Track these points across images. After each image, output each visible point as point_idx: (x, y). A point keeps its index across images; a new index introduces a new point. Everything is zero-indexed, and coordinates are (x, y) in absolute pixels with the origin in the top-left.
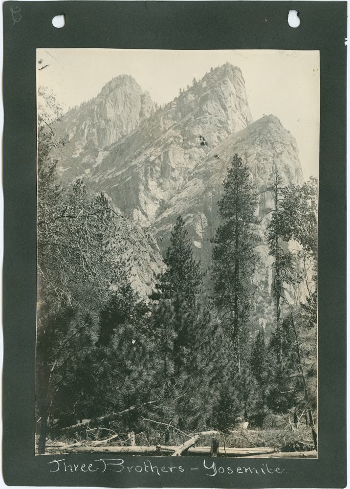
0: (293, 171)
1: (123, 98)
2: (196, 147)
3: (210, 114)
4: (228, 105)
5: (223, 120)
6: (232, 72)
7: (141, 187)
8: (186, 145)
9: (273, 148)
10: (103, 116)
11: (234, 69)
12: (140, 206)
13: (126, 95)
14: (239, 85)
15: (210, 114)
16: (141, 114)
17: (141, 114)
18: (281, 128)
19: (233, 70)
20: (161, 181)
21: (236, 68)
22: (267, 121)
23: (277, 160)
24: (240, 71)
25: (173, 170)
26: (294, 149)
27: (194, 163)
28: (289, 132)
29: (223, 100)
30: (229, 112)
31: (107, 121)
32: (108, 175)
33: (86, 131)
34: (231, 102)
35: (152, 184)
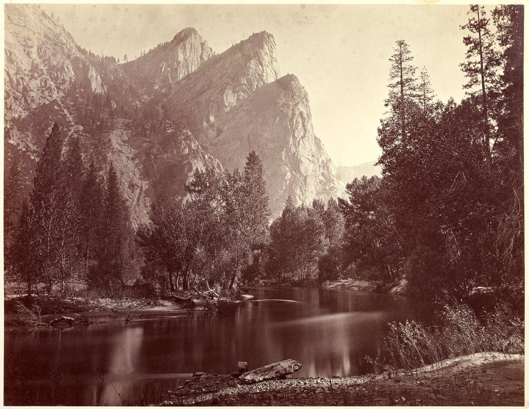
0: (305, 116)
1: (190, 46)
3: (252, 69)
4: (263, 63)
5: (260, 73)
6: (267, 39)
9: (294, 99)
10: (175, 59)
11: (270, 35)
13: (191, 45)
14: (272, 47)
15: (252, 69)
16: (201, 57)
17: (201, 57)
18: (298, 85)
19: (268, 37)
21: (270, 34)
24: (273, 37)
26: (306, 100)
28: (304, 88)
30: (264, 68)
34: (266, 59)
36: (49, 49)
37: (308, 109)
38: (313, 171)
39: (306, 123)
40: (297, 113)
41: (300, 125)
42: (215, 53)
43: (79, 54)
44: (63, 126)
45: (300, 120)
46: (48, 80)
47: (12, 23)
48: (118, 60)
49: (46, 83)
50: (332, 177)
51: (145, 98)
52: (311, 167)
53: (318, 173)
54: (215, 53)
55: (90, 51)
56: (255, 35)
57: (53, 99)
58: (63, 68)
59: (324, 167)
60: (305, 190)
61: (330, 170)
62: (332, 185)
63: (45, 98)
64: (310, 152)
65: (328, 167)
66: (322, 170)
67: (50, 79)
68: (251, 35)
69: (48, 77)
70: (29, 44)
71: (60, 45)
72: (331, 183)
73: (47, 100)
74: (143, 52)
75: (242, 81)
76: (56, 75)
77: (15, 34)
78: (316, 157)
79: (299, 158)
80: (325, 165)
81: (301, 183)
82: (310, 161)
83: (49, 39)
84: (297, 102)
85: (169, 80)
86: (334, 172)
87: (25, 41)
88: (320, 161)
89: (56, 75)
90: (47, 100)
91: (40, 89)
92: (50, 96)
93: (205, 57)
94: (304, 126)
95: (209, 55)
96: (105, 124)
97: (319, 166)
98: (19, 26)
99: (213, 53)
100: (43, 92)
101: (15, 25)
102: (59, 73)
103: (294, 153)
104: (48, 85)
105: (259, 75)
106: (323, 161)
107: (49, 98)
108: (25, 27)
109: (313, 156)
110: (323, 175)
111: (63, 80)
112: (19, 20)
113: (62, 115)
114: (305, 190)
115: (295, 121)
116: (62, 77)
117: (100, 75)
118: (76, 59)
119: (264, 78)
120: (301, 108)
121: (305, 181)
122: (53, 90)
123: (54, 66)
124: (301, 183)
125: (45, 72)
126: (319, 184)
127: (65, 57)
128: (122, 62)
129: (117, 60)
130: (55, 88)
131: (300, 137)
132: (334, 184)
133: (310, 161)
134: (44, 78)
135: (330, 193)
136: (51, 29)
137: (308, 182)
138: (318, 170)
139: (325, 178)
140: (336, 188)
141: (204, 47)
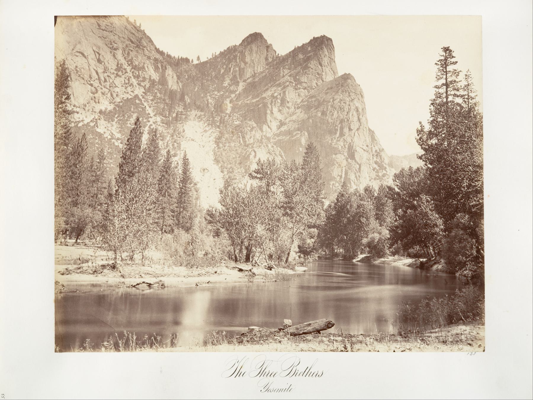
0: (360, 110)
2: (303, 88)
3: (312, 69)
4: (323, 63)
5: (320, 72)
7: (269, 112)
8: (296, 87)
9: (350, 96)
12: (267, 123)
15: (312, 69)
18: (354, 83)
20: (281, 108)
22: (346, 77)
23: (351, 104)
25: (288, 102)
27: (301, 99)
28: (359, 85)
29: (320, 60)
30: (323, 68)
31: (246, 63)
32: (247, 101)
33: (232, 69)
34: (326, 60)
35: (275, 110)
36: (132, 51)
37: (363, 104)
38: (367, 159)
39: (361, 117)
40: (353, 108)
41: (356, 119)
42: (278, 54)
43: (158, 56)
44: (143, 117)
45: (355, 113)
46: (131, 77)
47: (100, 29)
48: (192, 61)
49: (129, 80)
50: (385, 165)
51: (216, 94)
52: (365, 155)
53: (371, 161)
54: (278, 54)
55: (167, 53)
56: (315, 39)
57: (136, 94)
58: (143, 68)
59: (377, 155)
60: (359, 176)
61: (383, 159)
62: (384, 172)
63: (128, 93)
64: (365, 142)
65: (380, 156)
66: (375, 159)
67: (132, 77)
68: (312, 38)
69: (131, 75)
70: (114, 47)
71: (141, 47)
72: (383, 170)
73: (130, 95)
74: (214, 53)
75: (303, 79)
76: (137, 73)
77: (102, 38)
78: (370, 147)
79: (354, 148)
80: (378, 154)
81: (356, 170)
82: (364, 150)
83: (132, 42)
84: (353, 98)
85: (237, 78)
86: (386, 161)
87: (111, 44)
88: (374, 150)
89: (137, 73)
90: (130, 95)
91: (124, 85)
92: (132, 92)
93: (269, 59)
94: (359, 120)
95: (274, 57)
96: (180, 116)
97: (373, 155)
98: (106, 31)
99: (277, 54)
100: (126, 88)
101: (103, 30)
102: (140, 72)
103: (350, 143)
104: (131, 82)
105: (318, 74)
106: (376, 151)
107: (132, 93)
108: (111, 32)
109: (367, 146)
110: (376, 163)
111: (144, 78)
112: (107, 26)
113: (142, 108)
114: (359, 176)
115: (351, 115)
116: (143, 76)
117: (176, 73)
118: (156, 60)
119: (324, 77)
120: (357, 103)
121: (360, 168)
122: (135, 86)
123: (136, 66)
124: (356, 170)
125: (128, 71)
126: (372, 171)
127: (146, 58)
128: (196, 62)
129: (191, 60)
130: (137, 85)
131: (356, 129)
132: (386, 171)
133: (364, 150)
134: (127, 76)
135: (383, 179)
136: (134, 34)
137: (362, 169)
138: (371, 158)
139: (379, 166)
140: (388, 175)
141: (269, 50)
